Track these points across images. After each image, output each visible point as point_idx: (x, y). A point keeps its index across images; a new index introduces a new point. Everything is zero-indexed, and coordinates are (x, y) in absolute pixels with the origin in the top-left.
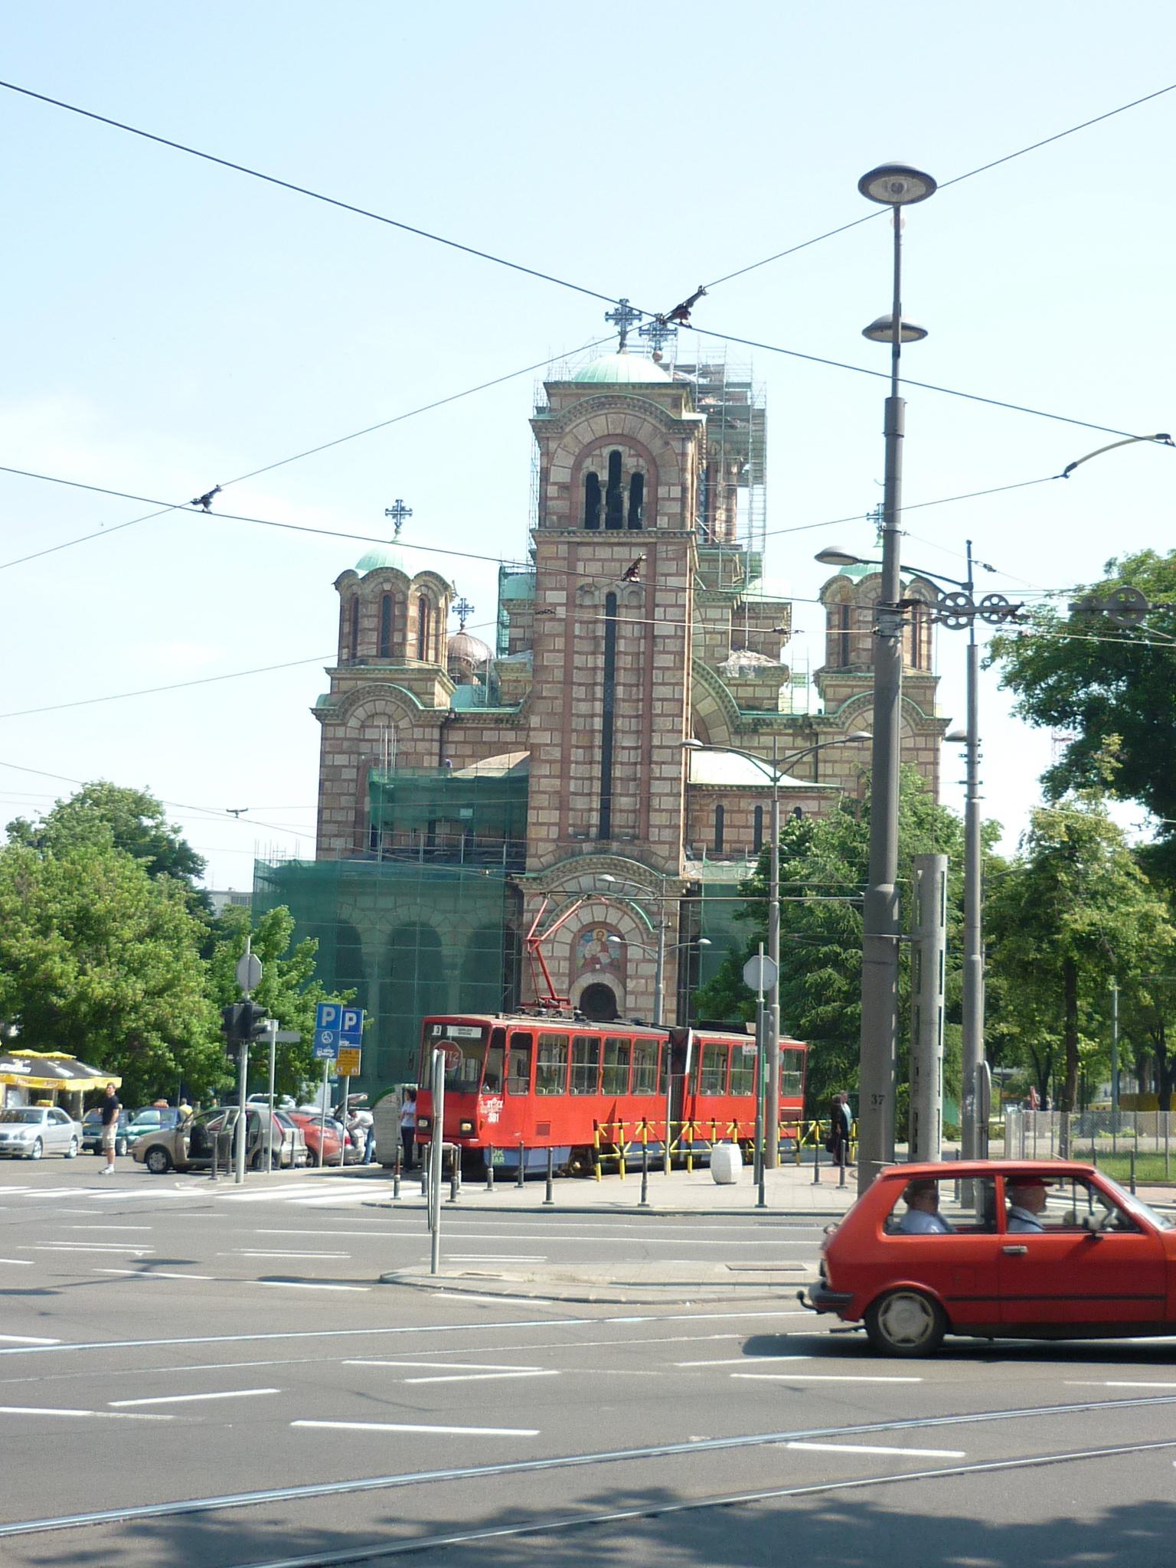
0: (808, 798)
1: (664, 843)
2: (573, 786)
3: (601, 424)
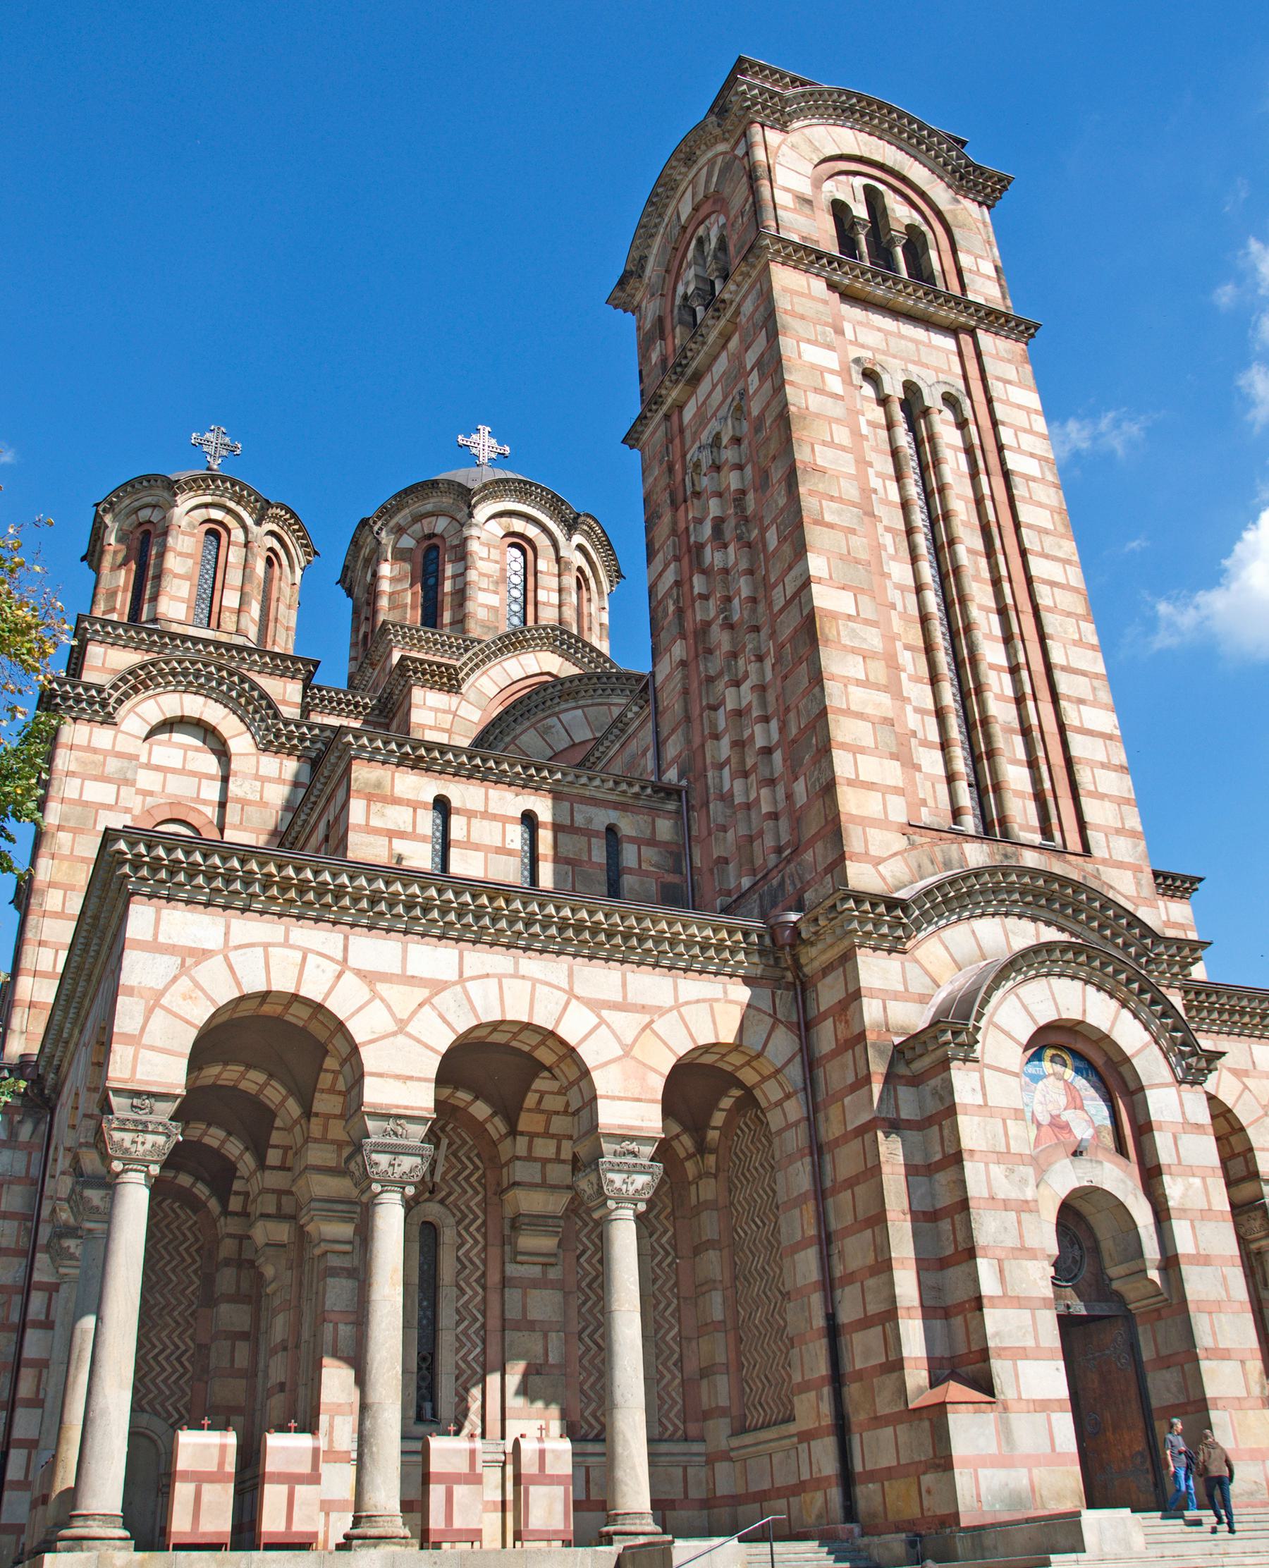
1: (1120, 865)
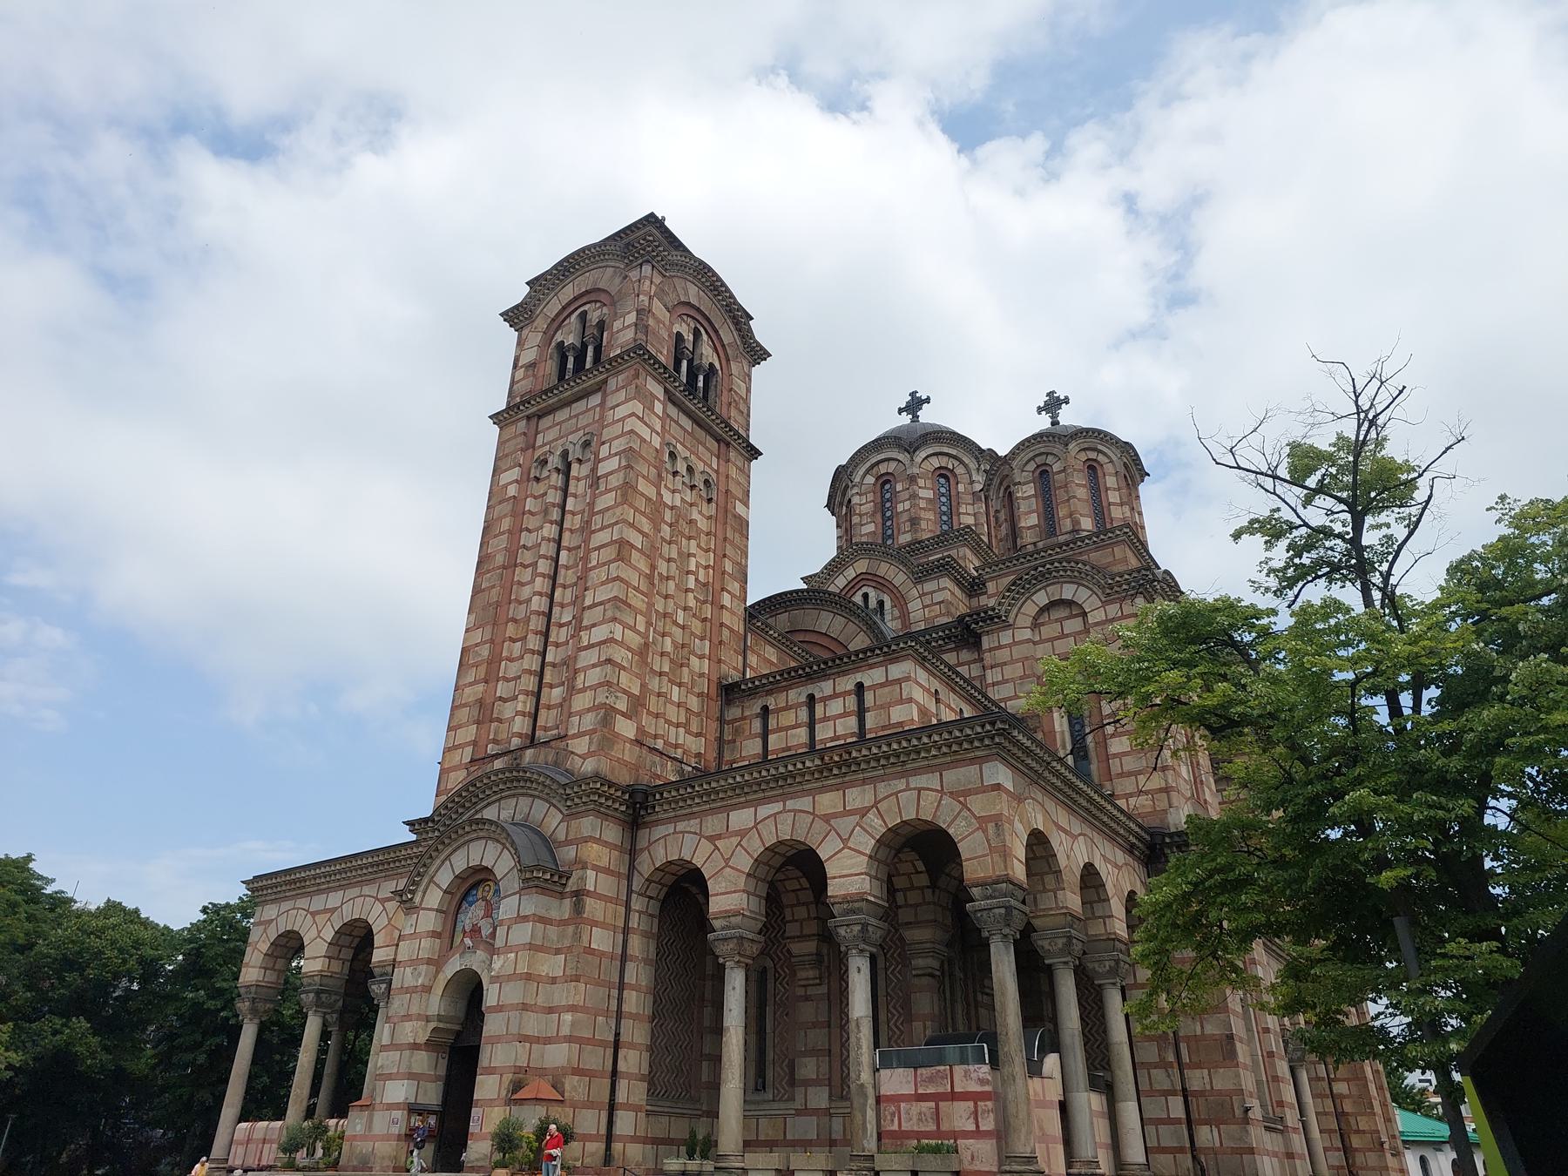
0: (871, 667)
2: (502, 689)
3: (568, 293)
